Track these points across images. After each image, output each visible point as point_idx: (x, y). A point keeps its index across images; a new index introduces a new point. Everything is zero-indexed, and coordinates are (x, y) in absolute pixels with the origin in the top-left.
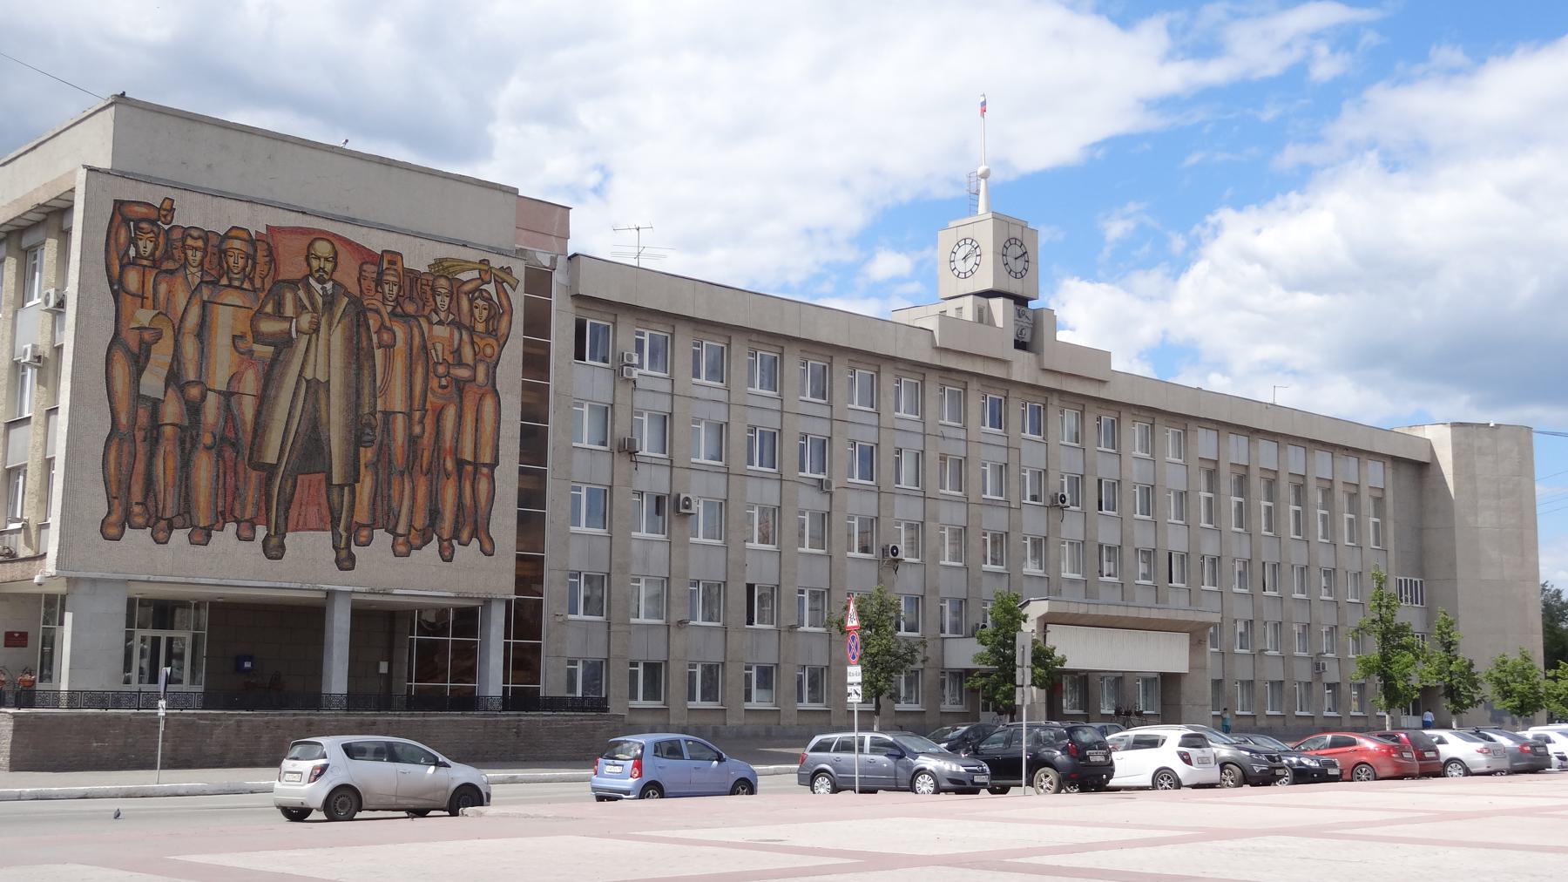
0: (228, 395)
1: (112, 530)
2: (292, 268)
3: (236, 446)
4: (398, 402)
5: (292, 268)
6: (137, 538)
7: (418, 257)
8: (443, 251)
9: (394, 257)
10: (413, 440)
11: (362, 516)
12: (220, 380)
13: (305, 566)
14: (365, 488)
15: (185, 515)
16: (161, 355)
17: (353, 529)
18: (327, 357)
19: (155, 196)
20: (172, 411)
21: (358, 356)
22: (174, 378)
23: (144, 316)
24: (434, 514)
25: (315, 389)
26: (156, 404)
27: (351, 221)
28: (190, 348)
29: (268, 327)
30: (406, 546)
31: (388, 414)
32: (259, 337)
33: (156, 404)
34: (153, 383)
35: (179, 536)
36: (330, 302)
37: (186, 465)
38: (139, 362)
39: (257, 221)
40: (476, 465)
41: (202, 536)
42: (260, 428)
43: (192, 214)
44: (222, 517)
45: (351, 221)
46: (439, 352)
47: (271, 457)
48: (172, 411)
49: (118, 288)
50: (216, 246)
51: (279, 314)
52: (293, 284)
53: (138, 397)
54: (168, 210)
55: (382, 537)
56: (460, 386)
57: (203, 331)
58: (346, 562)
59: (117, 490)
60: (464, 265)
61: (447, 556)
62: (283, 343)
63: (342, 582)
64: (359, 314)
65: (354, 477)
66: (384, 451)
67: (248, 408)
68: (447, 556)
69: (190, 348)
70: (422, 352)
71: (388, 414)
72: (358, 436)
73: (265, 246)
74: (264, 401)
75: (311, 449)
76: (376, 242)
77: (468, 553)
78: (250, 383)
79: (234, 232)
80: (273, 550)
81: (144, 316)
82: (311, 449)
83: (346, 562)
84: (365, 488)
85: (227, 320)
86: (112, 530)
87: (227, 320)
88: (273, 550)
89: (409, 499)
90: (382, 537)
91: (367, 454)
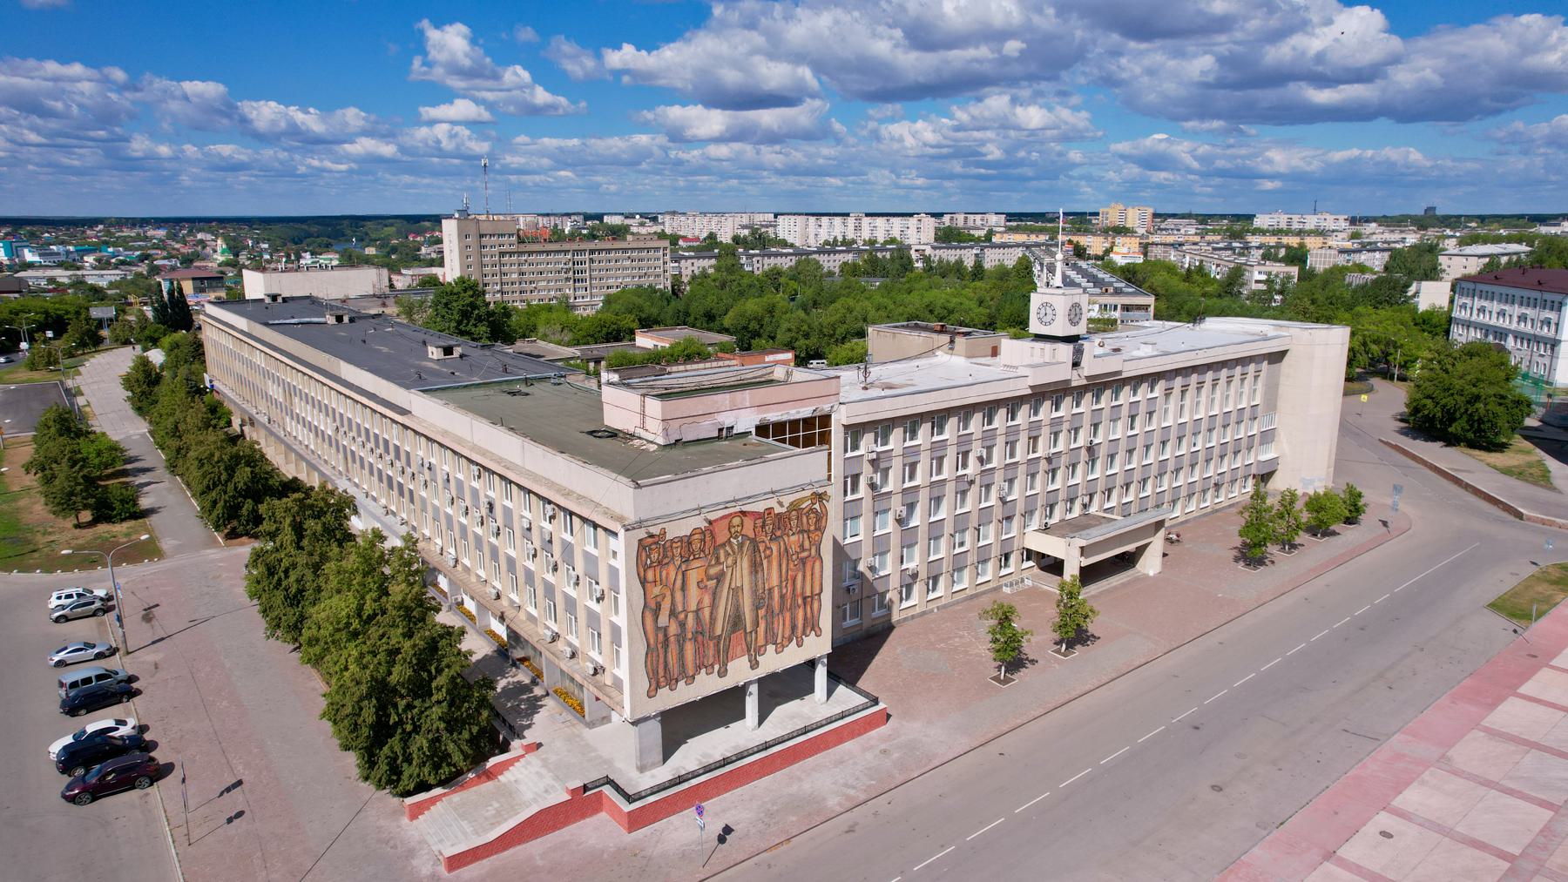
0: (697, 612)
2: (721, 539)
4: (775, 581)
5: (722, 537)
10: (782, 597)
11: (761, 641)
12: (693, 607)
14: (762, 626)
16: (666, 606)
18: (741, 575)
20: (673, 629)
21: (756, 567)
22: (673, 613)
23: (657, 590)
24: (794, 628)
26: (666, 629)
28: (678, 595)
29: (713, 571)
32: (710, 578)
35: (681, 684)
36: (741, 545)
44: (698, 668)
46: (794, 548)
47: (718, 632)
48: (673, 629)
49: (643, 582)
52: (723, 545)
53: (658, 629)
55: (771, 648)
62: (719, 578)
64: (754, 541)
66: (770, 612)
67: (707, 612)
69: (678, 595)
74: (713, 606)
75: (736, 622)
76: (760, 507)
78: (707, 601)
81: (657, 590)
82: (736, 622)
83: (754, 665)
84: (762, 626)
87: (694, 577)
90: (771, 648)
91: (762, 612)
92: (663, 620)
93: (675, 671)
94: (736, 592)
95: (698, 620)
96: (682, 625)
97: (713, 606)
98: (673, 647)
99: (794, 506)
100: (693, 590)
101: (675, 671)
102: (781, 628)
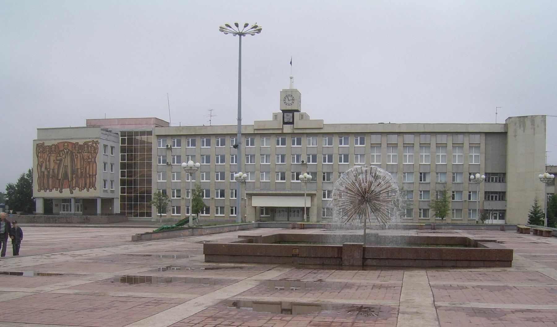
0: (53, 169)
1: (39, 191)
2: (61, 149)
3: (55, 177)
4: (79, 167)
6: (42, 191)
7: (81, 142)
10: (82, 173)
11: (74, 186)
12: (52, 168)
13: (66, 193)
14: (74, 181)
15: (48, 188)
16: (44, 165)
17: (73, 187)
18: (67, 161)
20: (46, 173)
21: (72, 160)
22: (46, 168)
24: (86, 184)
25: (66, 167)
26: (44, 172)
27: (72, 139)
28: (48, 163)
29: (58, 158)
30: (81, 190)
31: (77, 169)
32: (57, 160)
33: (44, 172)
34: (43, 169)
35: (48, 191)
36: (67, 153)
37: (48, 181)
38: (41, 166)
39: (56, 142)
40: (93, 175)
41: (51, 191)
43: (47, 144)
44: (53, 188)
45: (72, 139)
46: (85, 158)
48: (46, 173)
49: (38, 156)
50: (50, 147)
51: (60, 156)
52: (62, 151)
53: (41, 172)
54: (44, 143)
55: (77, 189)
56: (89, 163)
57: (49, 161)
58: (72, 193)
59: (39, 185)
60: (90, 142)
62: (61, 160)
64: (72, 153)
65: (72, 179)
67: (56, 171)
69: (48, 163)
70: (83, 158)
71: (77, 169)
72: (73, 173)
73: (57, 146)
74: (59, 169)
76: (74, 141)
77: (92, 190)
78: (56, 167)
80: (61, 192)
81: (41, 160)
83: (72, 193)
84: (74, 181)
85: (52, 158)
86: (39, 191)
87: (52, 158)
88: (61, 192)
89: (81, 182)
90: (77, 189)
91: (74, 176)
92: (43, 169)
93: (46, 186)
94: (66, 167)
95: (53, 172)
96: (49, 172)
97: (59, 169)
98: (46, 178)
99: (86, 143)
100: (52, 161)
101: (46, 186)
102: (81, 182)
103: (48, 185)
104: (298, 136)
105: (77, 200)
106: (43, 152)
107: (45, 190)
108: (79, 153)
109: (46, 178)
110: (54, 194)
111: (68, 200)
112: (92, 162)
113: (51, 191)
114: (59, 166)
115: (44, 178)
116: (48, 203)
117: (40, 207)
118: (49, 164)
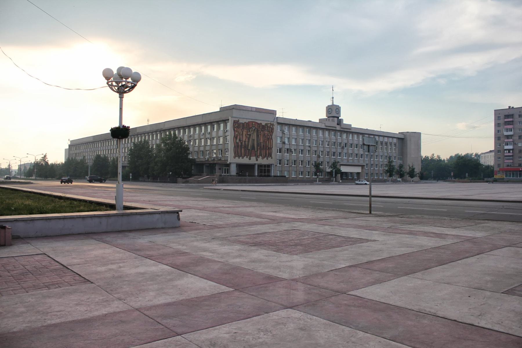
0: (245, 142)
1: (235, 157)
2: (251, 126)
3: (246, 147)
6: (237, 158)
7: (263, 124)
8: (266, 122)
9: (261, 124)
10: (263, 146)
12: (244, 140)
13: (253, 160)
15: (241, 156)
16: (238, 137)
18: (254, 136)
19: (237, 119)
20: (240, 144)
21: (258, 136)
22: (240, 140)
23: (237, 133)
24: (266, 154)
25: (253, 140)
29: (249, 133)
30: (263, 158)
34: (238, 141)
38: (236, 138)
39: (247, 121)
41: (243, 158)
42: (248, 145)
44: (245, 155)
46: (266, 135)
48: (240, 144)
49: (234, 130)
50: (243, 124)
54: (239, 121)
55: (261, 157)
56: (268, 138)
58: (257, 160)
59: (235, 153)
60: (268, 124)
61: (267, 159)
62: (250, 135)
63: (256, 162)
64: (258, 131)
66: (261, 147)
67: (247, 143)
68: (267, 159)
70: (264, 135)
72: (258, 146)
73: (248, 124)
74: (248, 142)
75: (253, 147)
76: (259, 122)
77: (270, 159)
78: (247, 140)
79: (245, 123)
80: (250, 159)
81: (237, 133)
82: (253, 147)
83: (257, 160)
85: (244, 133)
86: (235, 157)
87: (244, 133)
88: (250, 159)
89: (263, 152)
90: (261, 157)
94: (253, 140)
96: (242, 143)
97: (248, 142)
98: (239, 148)
99: (266, 124)
103: (241, 154)
104: (342, 132)
105: (260, 166)
106: (238, 127)
107: (239, 157)
108: (263, 131)
109: (239, 148)
110: (245, 161)
111: (252, 166)
112: (269, 139)
113: (243, 158)
114: (249, 139)
115: (238, 147)
116: (241, 167)
117: (233, 170)
118: (242, 137)
